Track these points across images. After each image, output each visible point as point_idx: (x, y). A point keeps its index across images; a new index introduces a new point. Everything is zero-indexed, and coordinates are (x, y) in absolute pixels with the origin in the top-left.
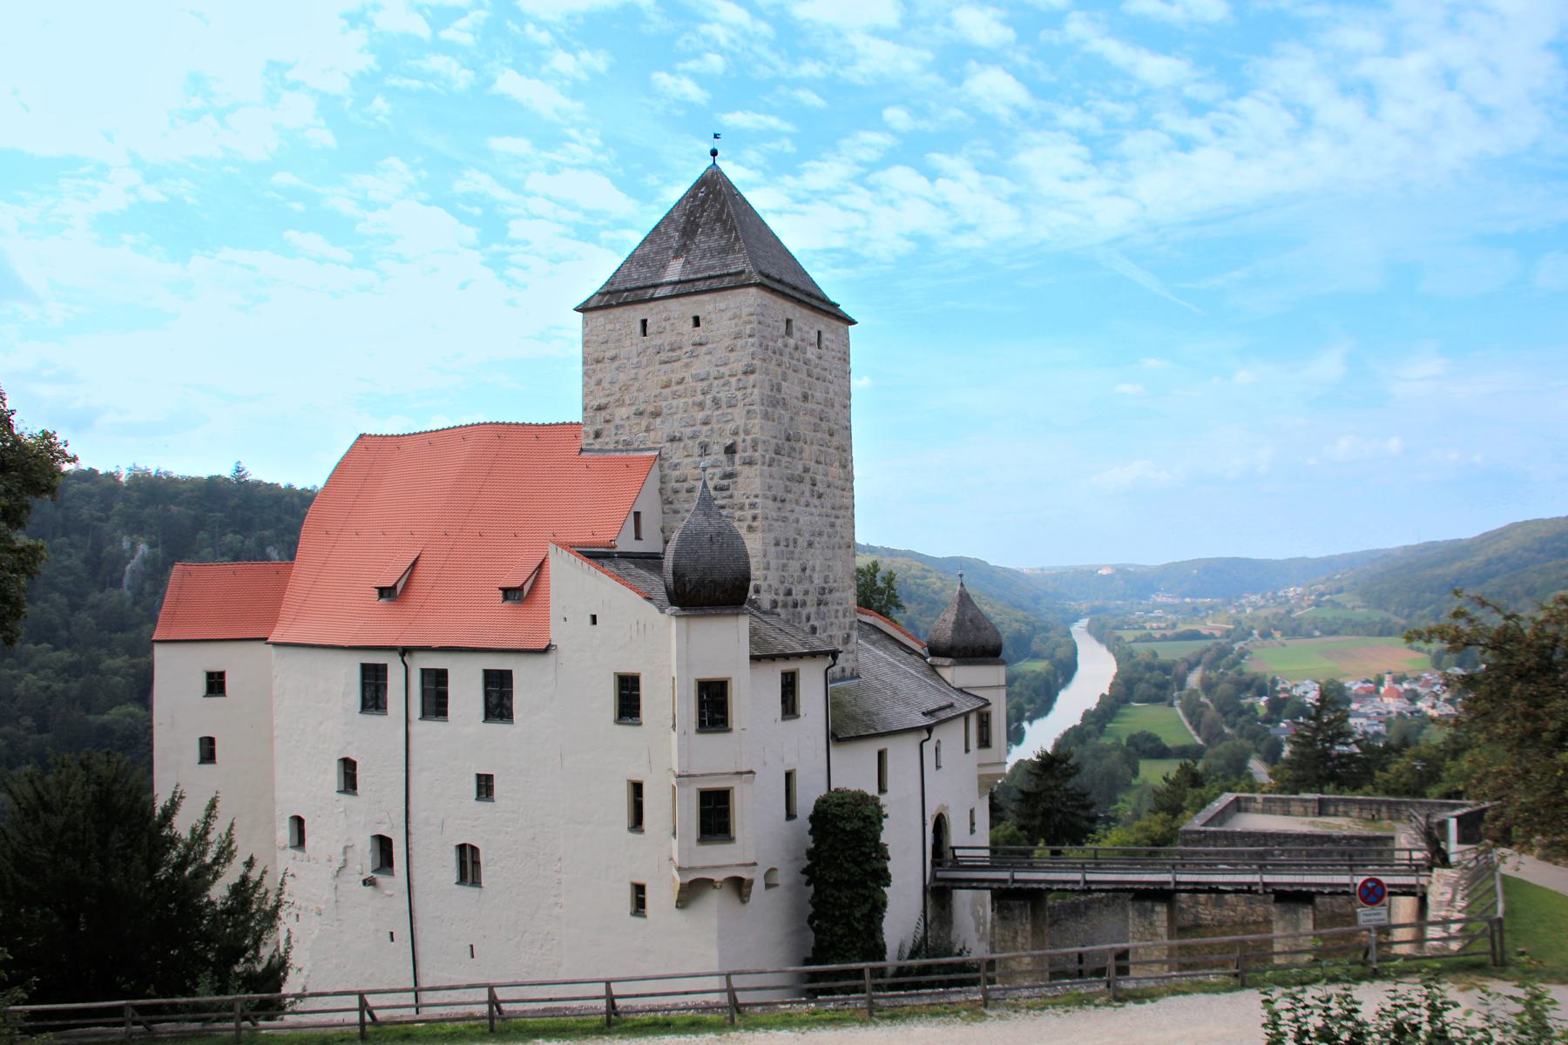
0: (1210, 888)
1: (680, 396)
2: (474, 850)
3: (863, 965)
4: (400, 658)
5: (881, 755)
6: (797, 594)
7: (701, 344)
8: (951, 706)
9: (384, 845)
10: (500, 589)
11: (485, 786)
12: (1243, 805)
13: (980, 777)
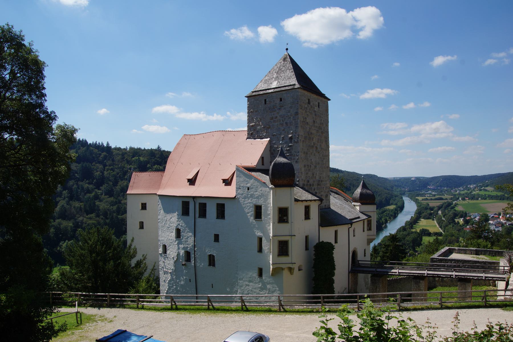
0: (438, 276)
1: (276, 122)
2: (213, 256)
3: (321, 295)
4: (193, 199)
5: (336, 232)
6: (311, 182)
7: (282, 106)
8: (359, 218)
9: (188, 255)
10: (222, 179)
11: (217, 238)
12: (451, 250)
13: (368, 239)
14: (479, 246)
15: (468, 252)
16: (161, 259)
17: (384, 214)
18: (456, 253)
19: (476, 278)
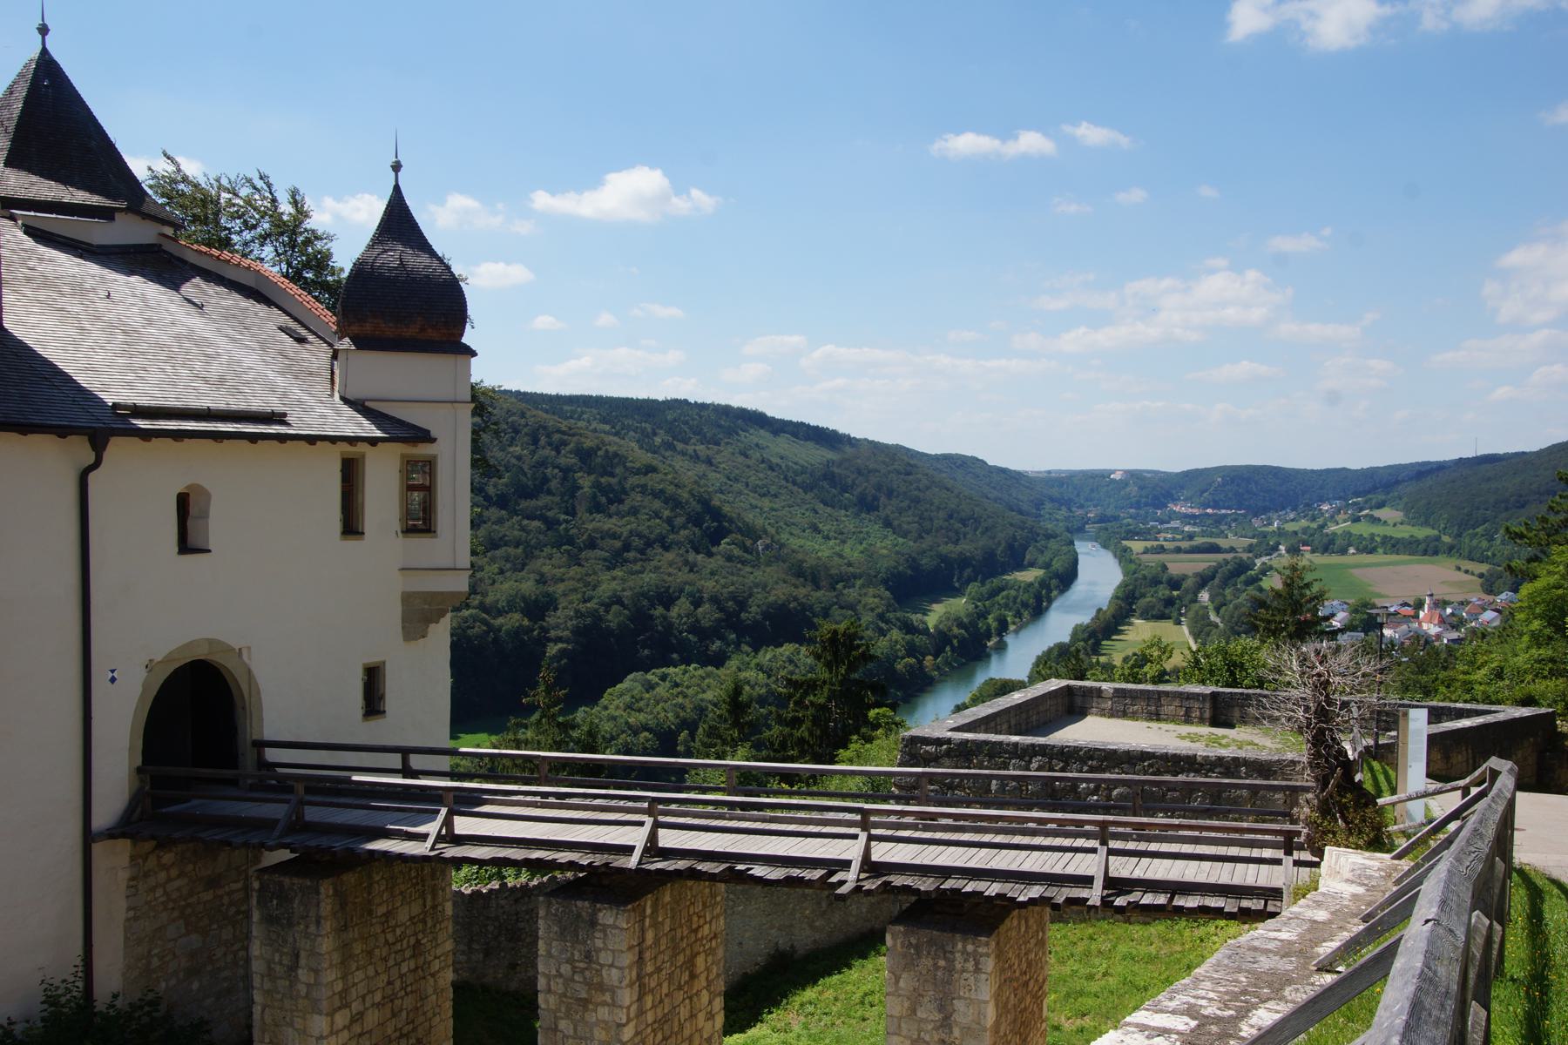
12: (1078, 701)
13: (407, 598)
14: (1232, 674)
15: (1168, 709)
17: (998, 598)
18: (1102, 713)
19: (1035, 891)
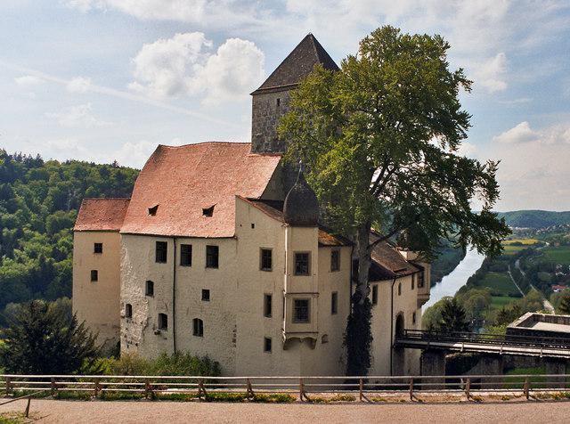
2: (201, 322)
9: (163, 318)
11: (206, 295)
13: (418, 300)
16: (123, 324)
